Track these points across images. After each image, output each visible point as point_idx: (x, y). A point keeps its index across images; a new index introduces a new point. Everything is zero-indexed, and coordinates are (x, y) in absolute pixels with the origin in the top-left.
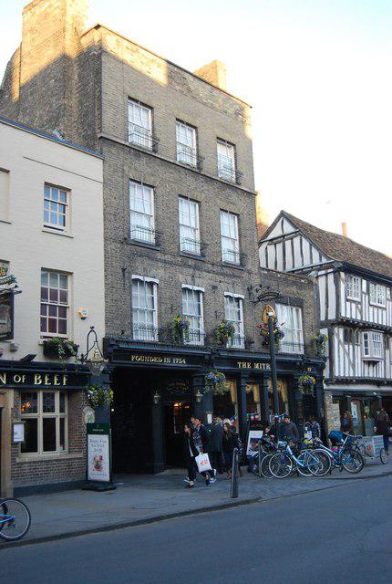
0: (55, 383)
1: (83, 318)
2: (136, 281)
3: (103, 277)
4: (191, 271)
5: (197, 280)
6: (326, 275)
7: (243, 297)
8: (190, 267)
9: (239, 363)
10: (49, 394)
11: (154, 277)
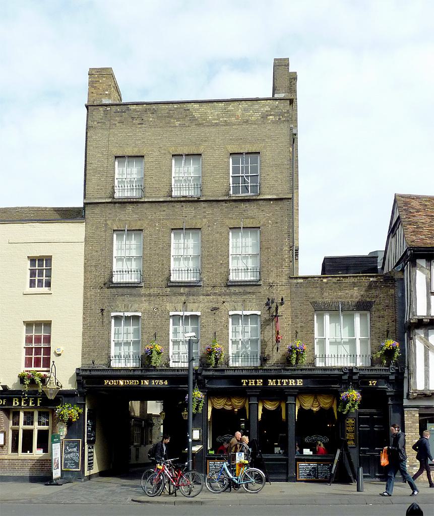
0: (22, 405)
1: (59, 355)
2: (116, 318)
4: (183, 298)
5: (190, 306)
7: (259, 313)
8: (182, 294)
9: (244, 381)
10: (29, 413)
11: (136, 311)
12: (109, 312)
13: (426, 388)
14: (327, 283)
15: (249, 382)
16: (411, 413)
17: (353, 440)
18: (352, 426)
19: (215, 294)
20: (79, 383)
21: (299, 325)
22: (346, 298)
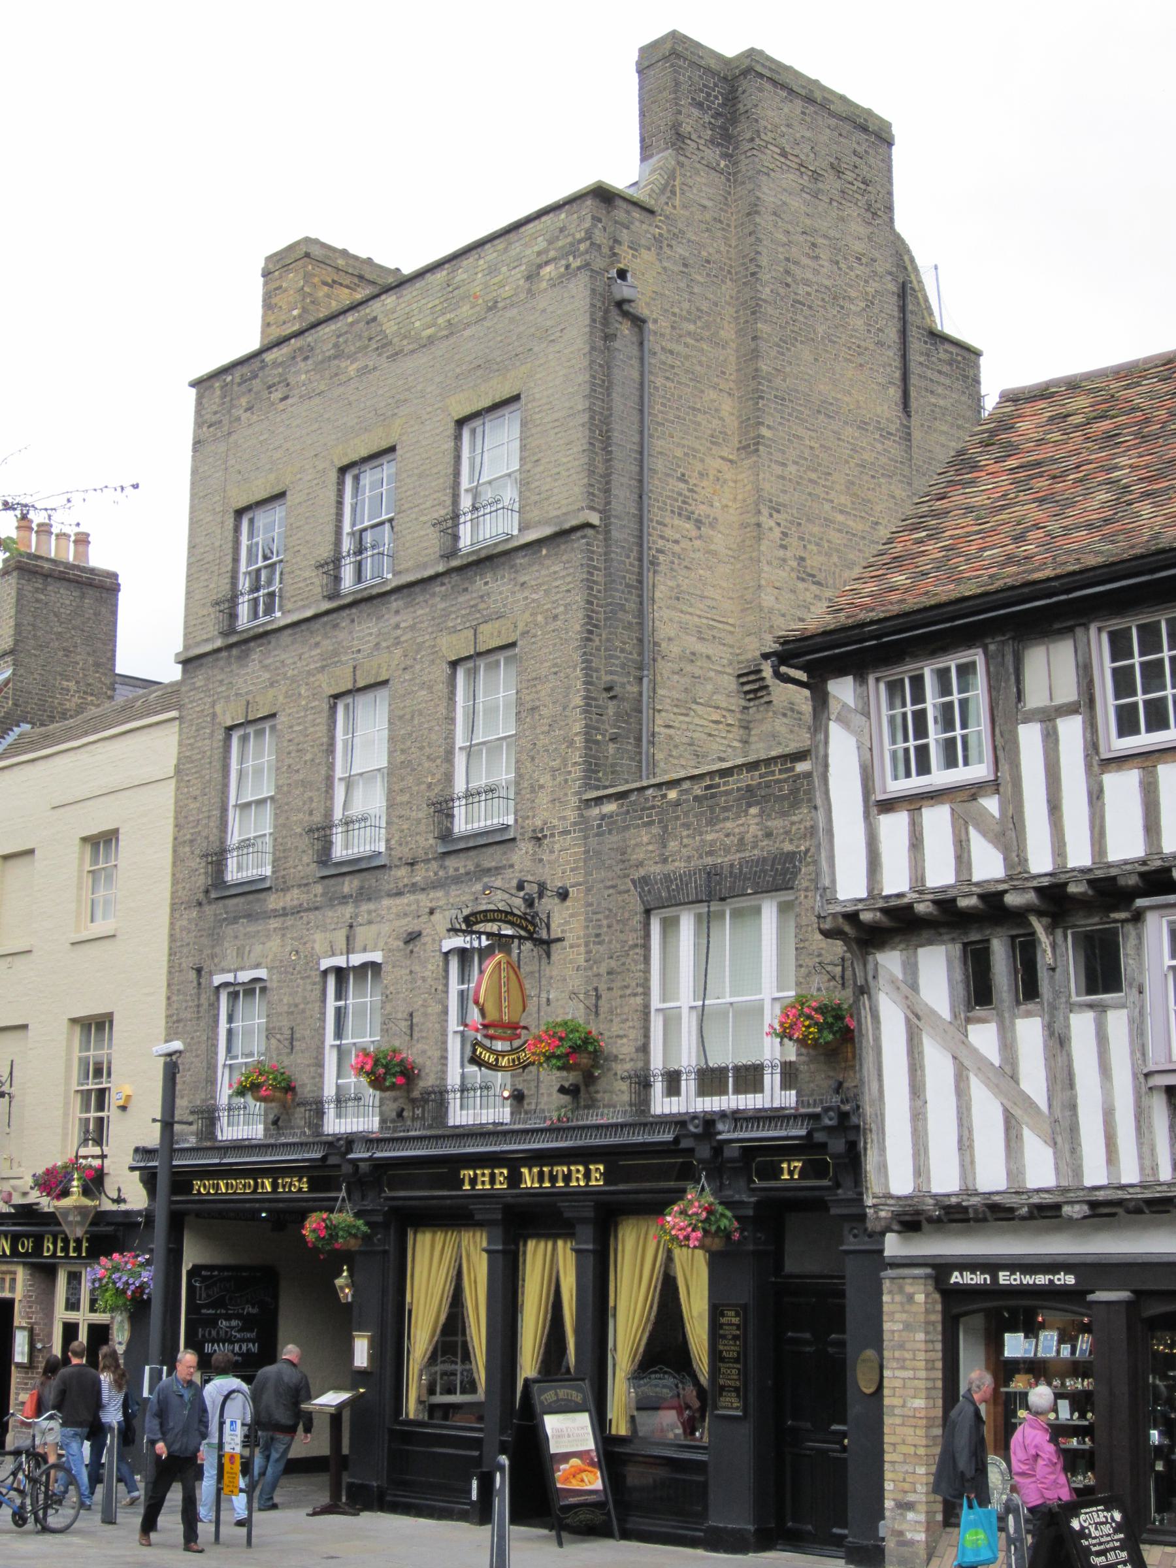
5: (361, 933)
8: (344, 899)
12: (211, 974)
13: (917, 1188)
14: (677, 804)
16: (901, 1290)
17: (737, 1390)
18: (735, 1338)
19: (414, 888)
21: (603, 969)
22: (727, 850)
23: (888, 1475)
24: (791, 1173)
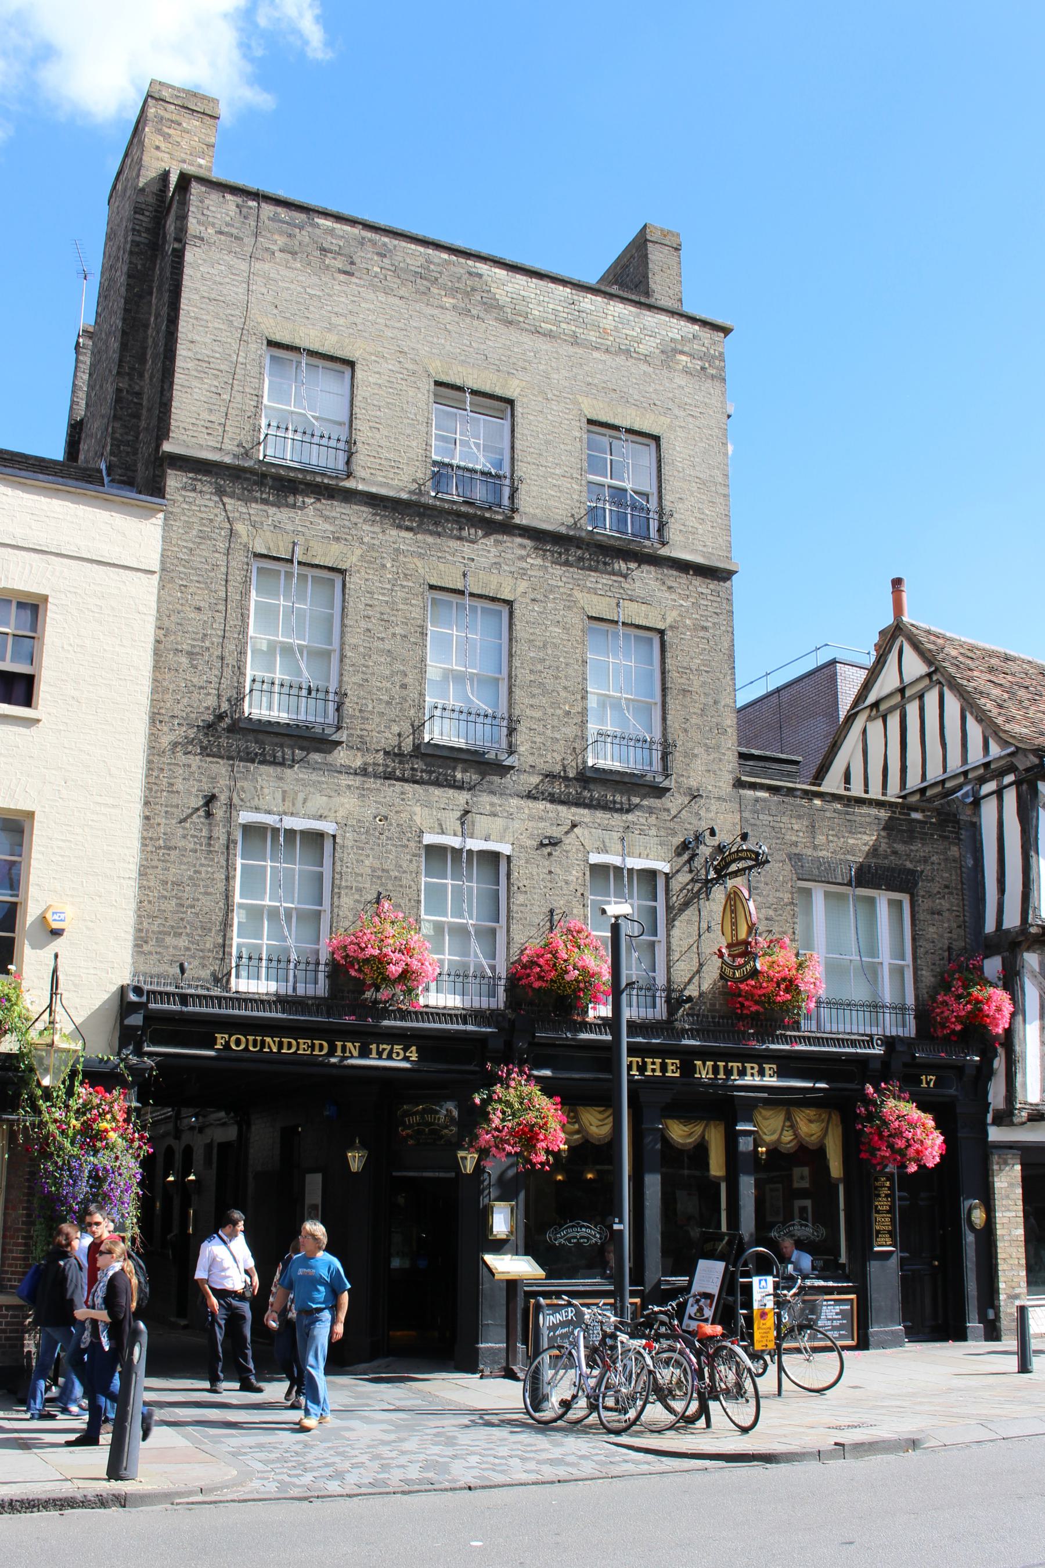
3: (137, 823)
4: (462, 798)
5: (482, 823)
6: (999, 793)
8: (459, 787)
15: (645, 1063)
17: (889, 1232)
18: (887, 1196)
20: (127, 1037)
23: (1001, 1279)
24: (928, 1083)
